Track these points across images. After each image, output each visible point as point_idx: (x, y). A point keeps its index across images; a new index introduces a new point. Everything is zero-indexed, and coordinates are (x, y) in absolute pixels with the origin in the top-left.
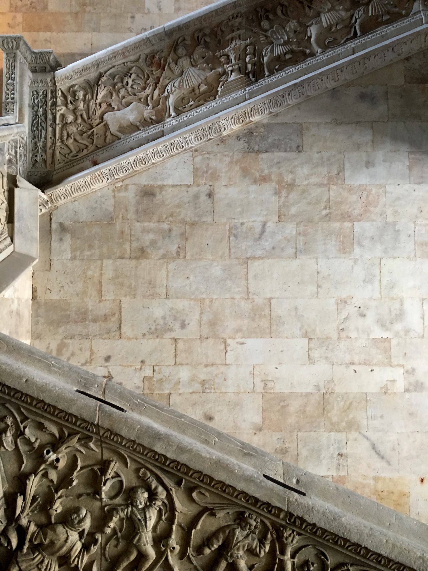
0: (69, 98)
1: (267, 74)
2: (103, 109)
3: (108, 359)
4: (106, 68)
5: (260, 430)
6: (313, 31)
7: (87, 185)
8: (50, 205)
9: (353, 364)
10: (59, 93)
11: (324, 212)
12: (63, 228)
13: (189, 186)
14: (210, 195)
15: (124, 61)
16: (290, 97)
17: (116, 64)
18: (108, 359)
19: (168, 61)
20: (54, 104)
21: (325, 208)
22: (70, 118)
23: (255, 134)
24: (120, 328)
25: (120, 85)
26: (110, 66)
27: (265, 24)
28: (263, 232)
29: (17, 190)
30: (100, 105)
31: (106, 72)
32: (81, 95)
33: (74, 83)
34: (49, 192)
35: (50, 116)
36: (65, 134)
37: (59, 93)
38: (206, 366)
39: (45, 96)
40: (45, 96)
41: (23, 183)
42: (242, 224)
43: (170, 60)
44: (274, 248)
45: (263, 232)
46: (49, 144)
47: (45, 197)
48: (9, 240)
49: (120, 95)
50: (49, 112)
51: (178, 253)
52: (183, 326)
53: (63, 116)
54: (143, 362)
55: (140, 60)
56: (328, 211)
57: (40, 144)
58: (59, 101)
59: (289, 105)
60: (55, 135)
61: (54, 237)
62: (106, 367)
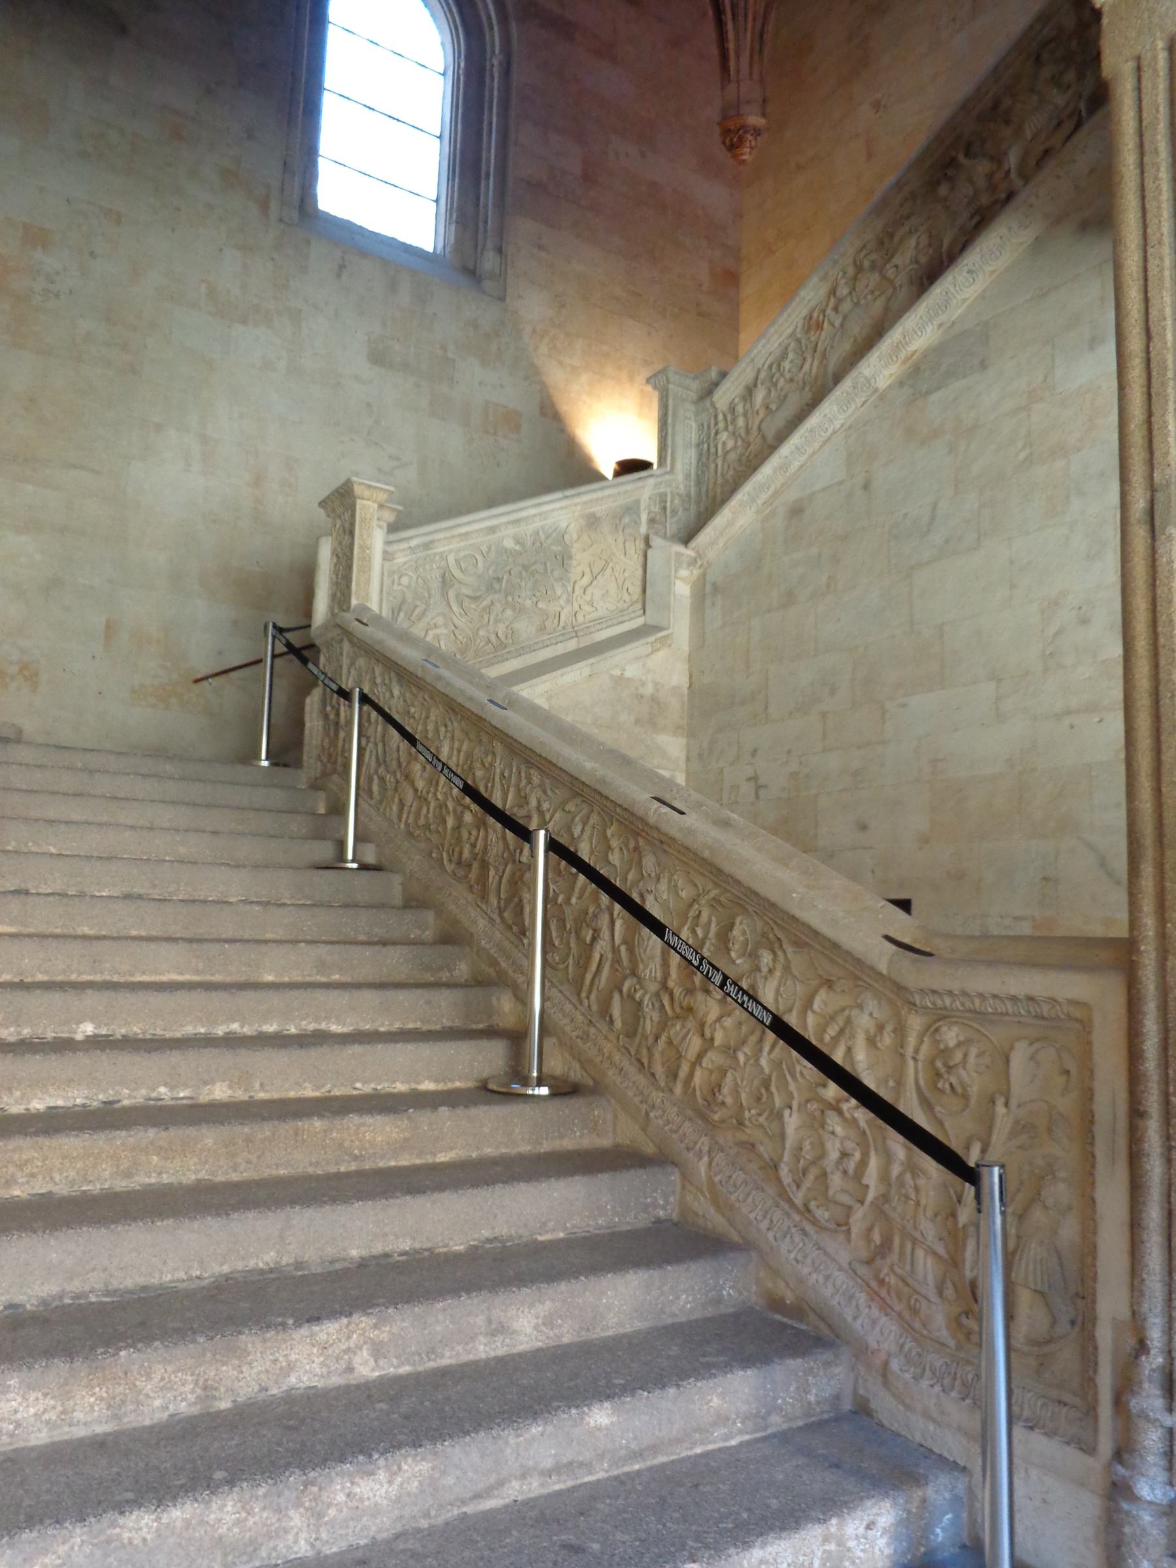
0: (729, 417)
1: (946, 264)
2: (761, 415)
3: (754, 753)
4: (763, 361)
5: (927, 842)
6: (1013, 159)
7: (730, 524)
8: (699, 563)
9: (1069, 712)
10: (721, 417)
11: (1022, 456)
12: (716, 588)
13: (841, 483)
14: (866, 487)
15: (781, 340)
16: (957, 288)
17: (772, 349)
18: (754, 753)
19: (827, 314)
20: (717, 433)
21: (1024, 448)
22: (730, 444)
23: (923, 368)
24: (766, 708)
25: (777, 375)
26: (767, 355)
27: (943, 190)
28: (933, 519)
29: (650, 552)
30: (758, 413)
31: (763, 365)
32: (740, 409)
33: (733, 396)
34: (693, 544)
35: (713, 450)
36: (726, 467)
37: (721, 417)
38: (859, 748)
39: (709, 426)
40: (709, 426)
41: (656, 541)
42: (906, 515)
43: (829, 311)
44: (947, 541)
45: (933, 519)
46: (711, 486)
47: (688, 552)
48: (642, 611)
49: (779, 388)
50: (712, 445)
51: (828, 586)
52: (833, 692)
53: (724, 444)
54: (789, 752)
55: (798, 330)
56: (1027, 451)
57: (704, 490)
58: (721, 425)
59: (964, 300)
60: (716, 472)
61: (708, 602)
62: (752, 764)
